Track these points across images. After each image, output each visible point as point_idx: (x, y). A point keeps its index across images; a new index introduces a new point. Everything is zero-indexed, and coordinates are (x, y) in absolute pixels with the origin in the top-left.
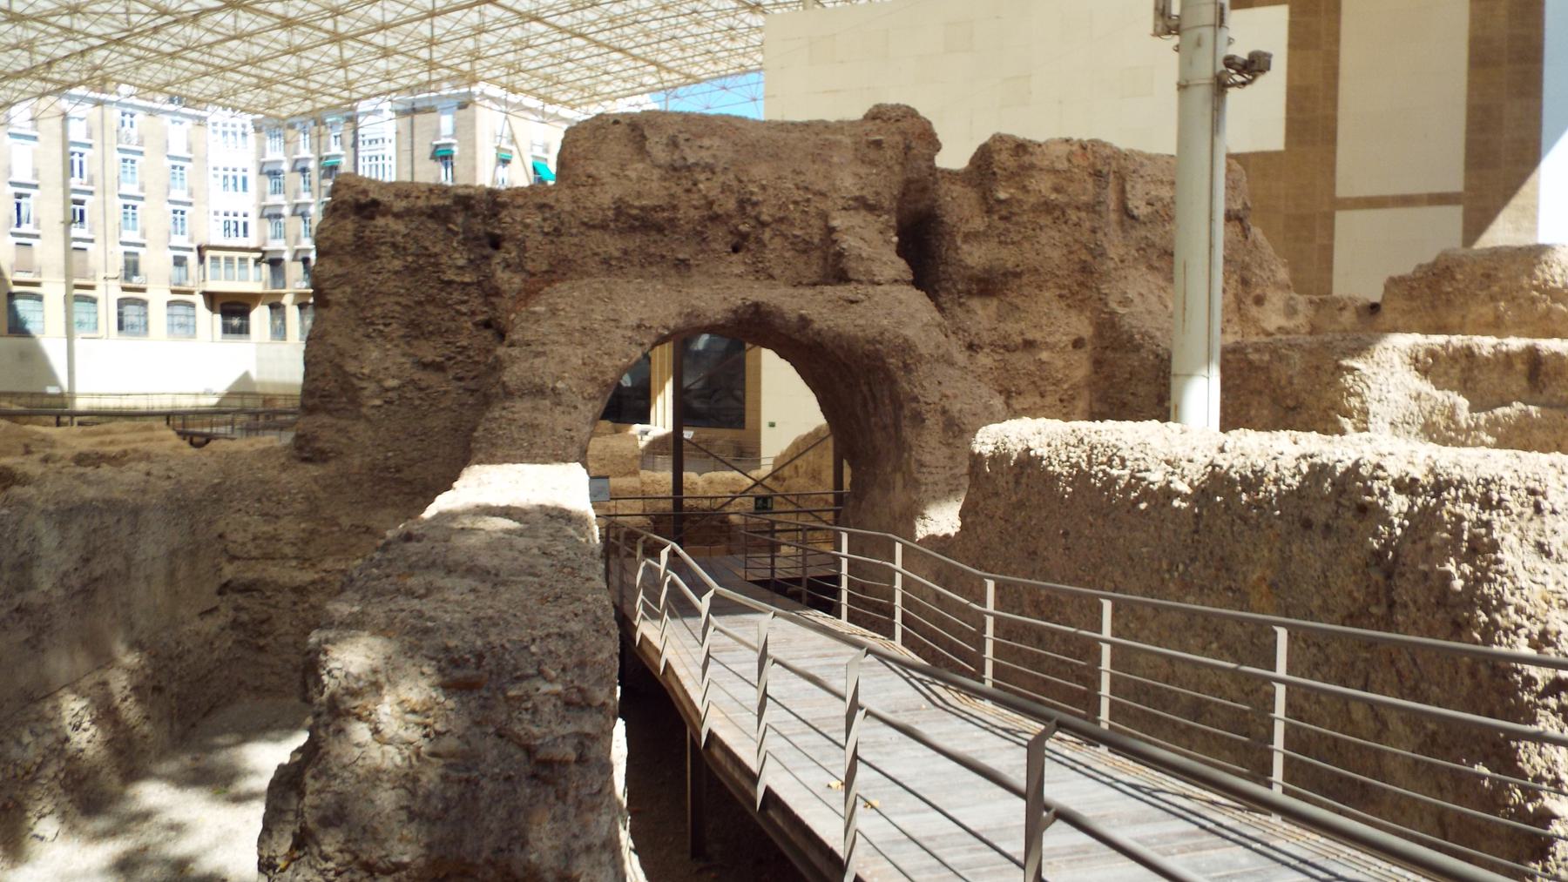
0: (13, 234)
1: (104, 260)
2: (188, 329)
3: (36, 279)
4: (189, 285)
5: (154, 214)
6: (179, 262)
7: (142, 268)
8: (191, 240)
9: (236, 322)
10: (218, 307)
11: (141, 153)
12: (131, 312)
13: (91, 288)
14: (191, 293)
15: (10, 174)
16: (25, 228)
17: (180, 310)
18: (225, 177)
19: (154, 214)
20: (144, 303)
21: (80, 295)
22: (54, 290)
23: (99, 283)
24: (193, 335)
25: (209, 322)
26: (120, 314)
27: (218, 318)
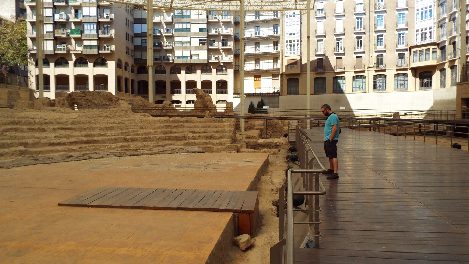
0: (335, 54)
1: (369, 59)
2: (404, 86)
3: (343, 71)
4: (404, 66)
5: (390, 38)
6: (401, 56)
7: (384, 61)
8: (407, 45)
9: (426, 81)
10: (418, 75)
11: (386, 11)
12: (380, 81)
13: (363, 72)
14: (406, 69)
15: (335, 31)
16: (341, 52)
17: (401, 78)
18: (422, 13)
19: (390, 38)
20: (385, 76)
21: (359, 75)
22: (349, 75)
23: (366, 69)
24: (407, 89)
25: (413, 81)
26: (374, 82)
27: (418, 80)
